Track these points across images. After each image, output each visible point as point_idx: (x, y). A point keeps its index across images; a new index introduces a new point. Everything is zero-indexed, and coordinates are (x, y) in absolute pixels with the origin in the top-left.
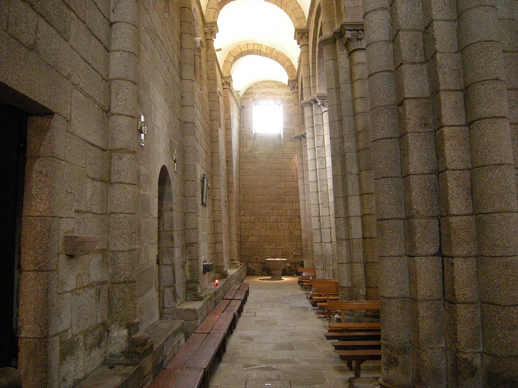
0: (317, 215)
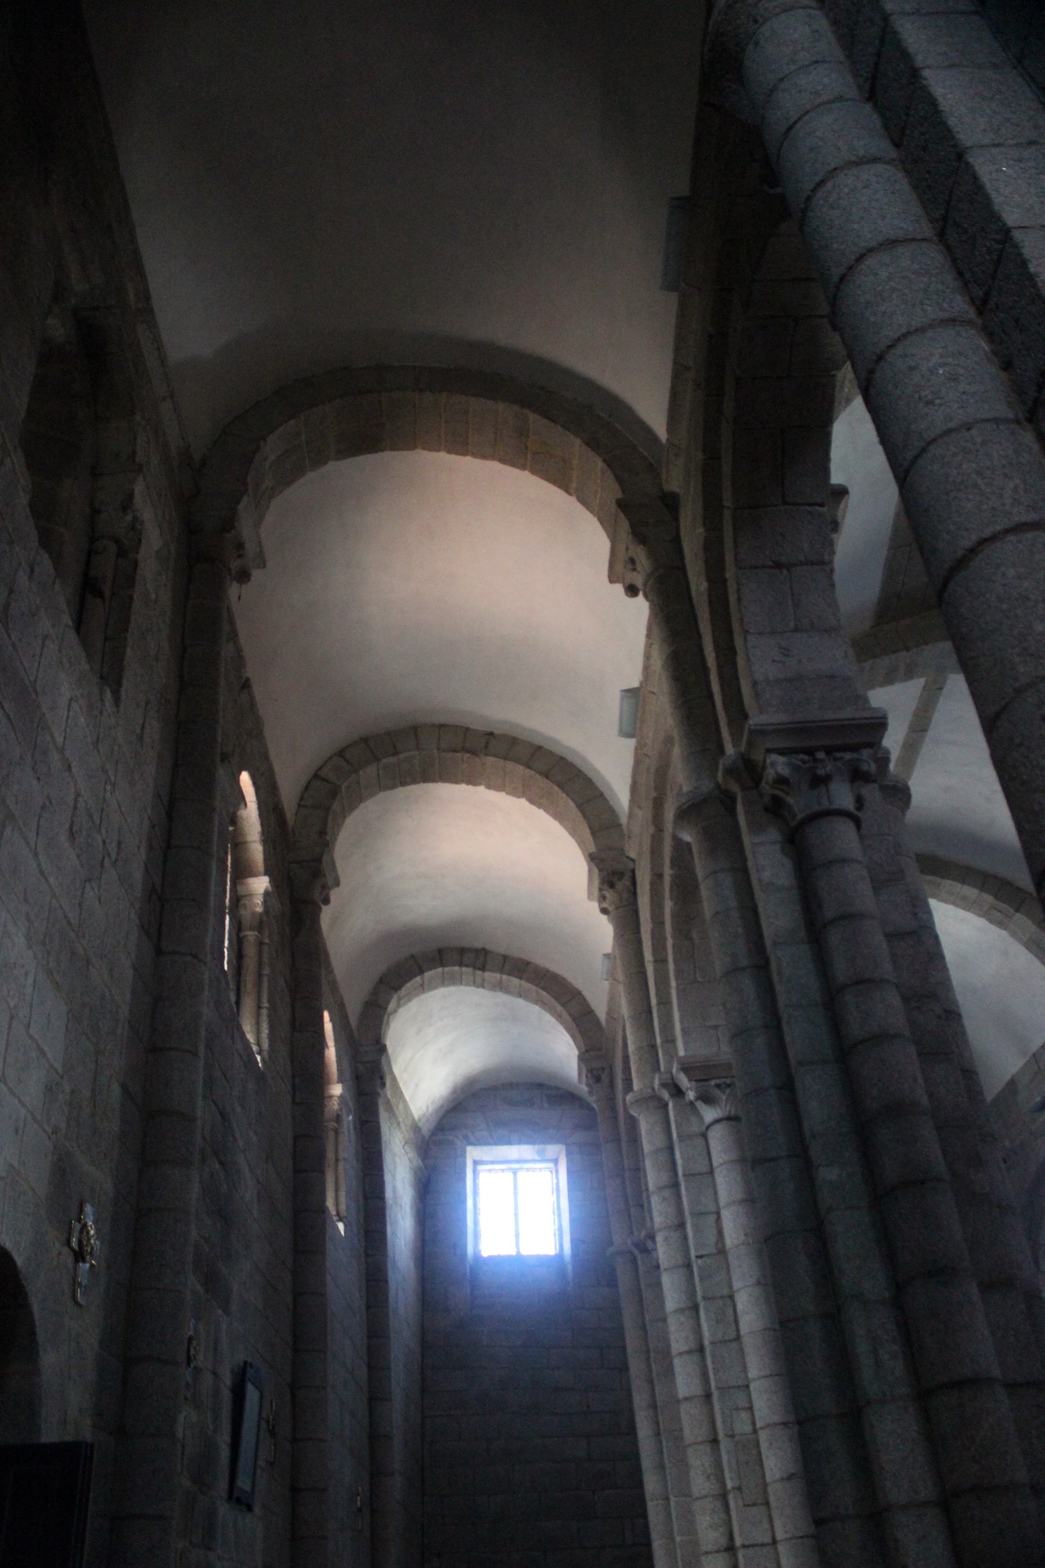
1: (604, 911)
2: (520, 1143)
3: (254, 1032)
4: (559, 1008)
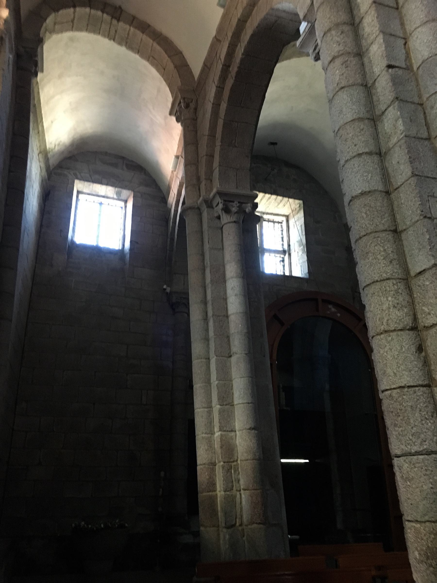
0: (408, 321)
2: (107, 184)
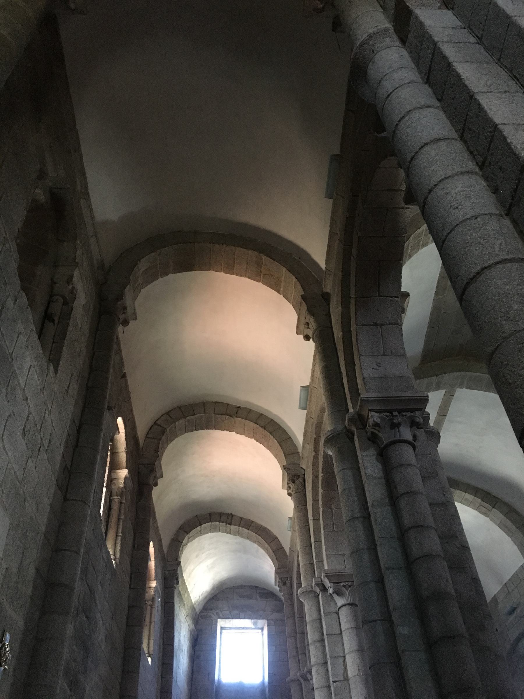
1: (289, 494)
3: (113, 548)
4: (267, 545)
